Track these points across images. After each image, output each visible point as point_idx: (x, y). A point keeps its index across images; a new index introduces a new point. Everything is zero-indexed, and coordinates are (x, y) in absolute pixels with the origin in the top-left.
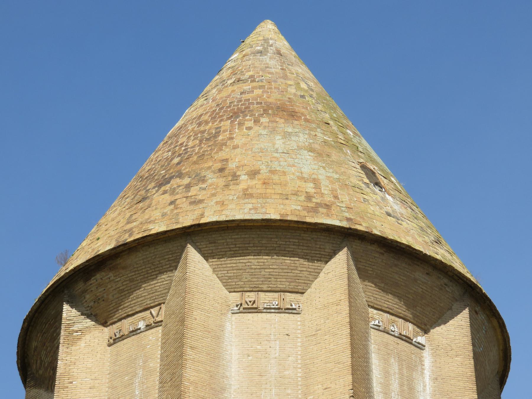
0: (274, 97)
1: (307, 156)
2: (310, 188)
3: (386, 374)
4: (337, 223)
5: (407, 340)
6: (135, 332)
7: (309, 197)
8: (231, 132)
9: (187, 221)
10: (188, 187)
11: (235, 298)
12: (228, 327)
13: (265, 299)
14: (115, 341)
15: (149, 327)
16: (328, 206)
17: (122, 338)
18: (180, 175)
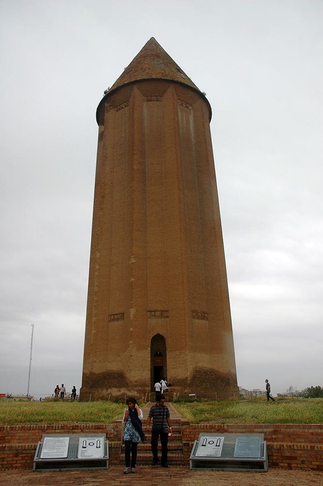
0: (154, 53)
1: (163, 65)
2: (163, 72)
3: (182, 115)
4: (169, 79)
5: (188, 108)
6: (123, 108)
7: (163, 74)
8: (144, 60)
9: (133, 80)
10: (134, 73)
11: (146, 98)
12: (144, 105)
13: (153, 98)
14: (117, 111)
15: (125, 107)
16: (167, 75)
17: (120, 110)
18: (132, 71)
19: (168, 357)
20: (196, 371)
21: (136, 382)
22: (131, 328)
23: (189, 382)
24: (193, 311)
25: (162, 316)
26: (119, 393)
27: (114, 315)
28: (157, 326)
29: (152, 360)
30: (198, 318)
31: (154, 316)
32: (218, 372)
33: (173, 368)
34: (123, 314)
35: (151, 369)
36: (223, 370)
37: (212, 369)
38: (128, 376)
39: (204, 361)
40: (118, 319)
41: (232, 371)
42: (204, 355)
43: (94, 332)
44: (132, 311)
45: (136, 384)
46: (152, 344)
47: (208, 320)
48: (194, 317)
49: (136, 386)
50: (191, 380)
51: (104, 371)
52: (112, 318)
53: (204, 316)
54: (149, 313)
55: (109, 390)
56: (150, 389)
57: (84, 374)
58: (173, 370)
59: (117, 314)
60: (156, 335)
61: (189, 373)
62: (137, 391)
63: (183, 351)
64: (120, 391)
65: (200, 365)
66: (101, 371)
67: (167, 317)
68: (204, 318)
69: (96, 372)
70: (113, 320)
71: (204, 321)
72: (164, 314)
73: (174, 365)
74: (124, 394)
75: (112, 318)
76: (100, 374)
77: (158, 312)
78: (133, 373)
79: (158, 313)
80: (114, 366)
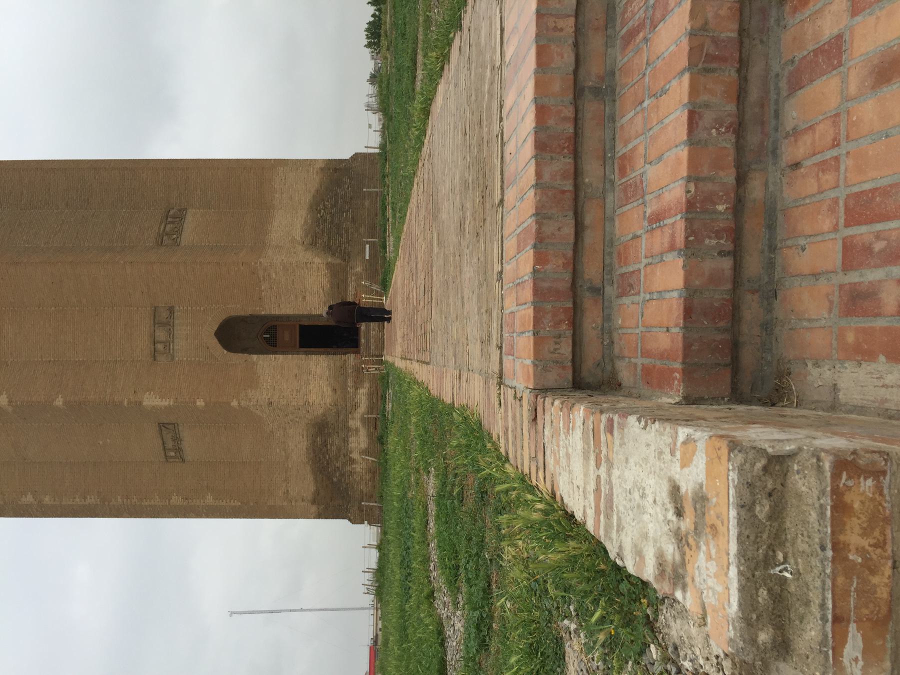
19: (276, 311)
20: (313, 244)
21: (335, 390)
22: (198, 403)
23: (338, 261)
24: (160, 243)
25: (168, 324)
26: (363, 432)
27: (164, 448)
28: (195, 335)
29: (285, 350)
30: (179, 232)
31: (167, 344)
32: (317, 191)
33: (304, 298)
34: (162, 426)
35: (307, 353)
36: (314, 181)
37: (311, 207)
38: (321, 411)
39: (290, 222)
40: (177, 439)
41: (318, 166)
42: (275, 224)
43: (210, 499)
44: (151, 401)
45: (339, 392)
46: (244, 350)
47: (186, 209)
48: (176, 243)
49: (344, 387)
50: (333, 255)
51: (308, 468)
52: (172, 454)
53: (175, 218)
54: (158, 358)
55: (355, 455)
56: (353, 356)
57: (319, 516)
58: (307, 298)
59: (164, 443)
60: (220, 341)
61: (317, 260)
62: (356, 389)
63: (261, 273)
64: (357, 430)
65: (298, 233)
66: (310, 477)
67: (171, 310)
68: (180, 217)
69: (312, 488)
70: (179, 450)
71: (189, 218)
72: (163, 319)
73: (296, 296)
74: (363, 420)
75: (172, 454)
76: (315, 479)
77: (157, 334)
78: (312, 398)
79: (161, 335)
80: (297, 445)
